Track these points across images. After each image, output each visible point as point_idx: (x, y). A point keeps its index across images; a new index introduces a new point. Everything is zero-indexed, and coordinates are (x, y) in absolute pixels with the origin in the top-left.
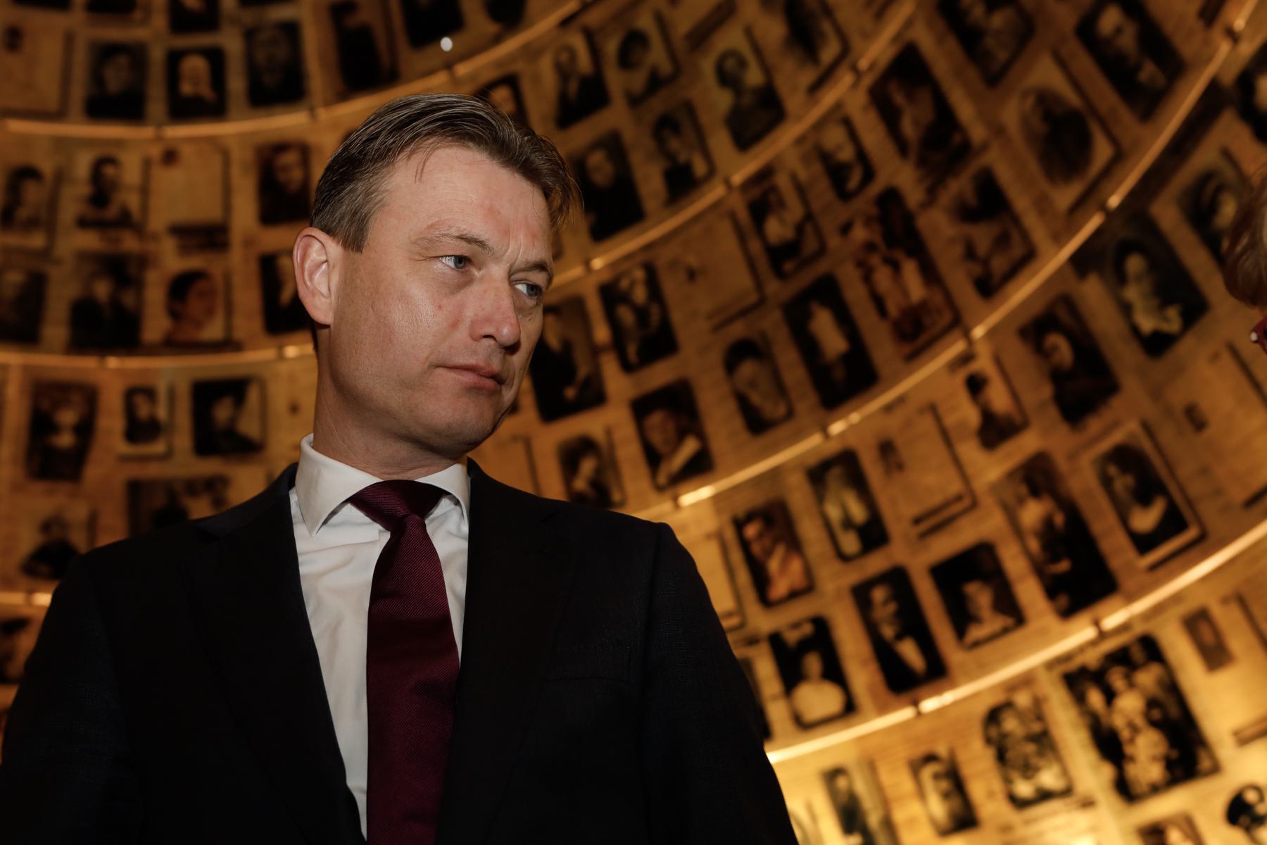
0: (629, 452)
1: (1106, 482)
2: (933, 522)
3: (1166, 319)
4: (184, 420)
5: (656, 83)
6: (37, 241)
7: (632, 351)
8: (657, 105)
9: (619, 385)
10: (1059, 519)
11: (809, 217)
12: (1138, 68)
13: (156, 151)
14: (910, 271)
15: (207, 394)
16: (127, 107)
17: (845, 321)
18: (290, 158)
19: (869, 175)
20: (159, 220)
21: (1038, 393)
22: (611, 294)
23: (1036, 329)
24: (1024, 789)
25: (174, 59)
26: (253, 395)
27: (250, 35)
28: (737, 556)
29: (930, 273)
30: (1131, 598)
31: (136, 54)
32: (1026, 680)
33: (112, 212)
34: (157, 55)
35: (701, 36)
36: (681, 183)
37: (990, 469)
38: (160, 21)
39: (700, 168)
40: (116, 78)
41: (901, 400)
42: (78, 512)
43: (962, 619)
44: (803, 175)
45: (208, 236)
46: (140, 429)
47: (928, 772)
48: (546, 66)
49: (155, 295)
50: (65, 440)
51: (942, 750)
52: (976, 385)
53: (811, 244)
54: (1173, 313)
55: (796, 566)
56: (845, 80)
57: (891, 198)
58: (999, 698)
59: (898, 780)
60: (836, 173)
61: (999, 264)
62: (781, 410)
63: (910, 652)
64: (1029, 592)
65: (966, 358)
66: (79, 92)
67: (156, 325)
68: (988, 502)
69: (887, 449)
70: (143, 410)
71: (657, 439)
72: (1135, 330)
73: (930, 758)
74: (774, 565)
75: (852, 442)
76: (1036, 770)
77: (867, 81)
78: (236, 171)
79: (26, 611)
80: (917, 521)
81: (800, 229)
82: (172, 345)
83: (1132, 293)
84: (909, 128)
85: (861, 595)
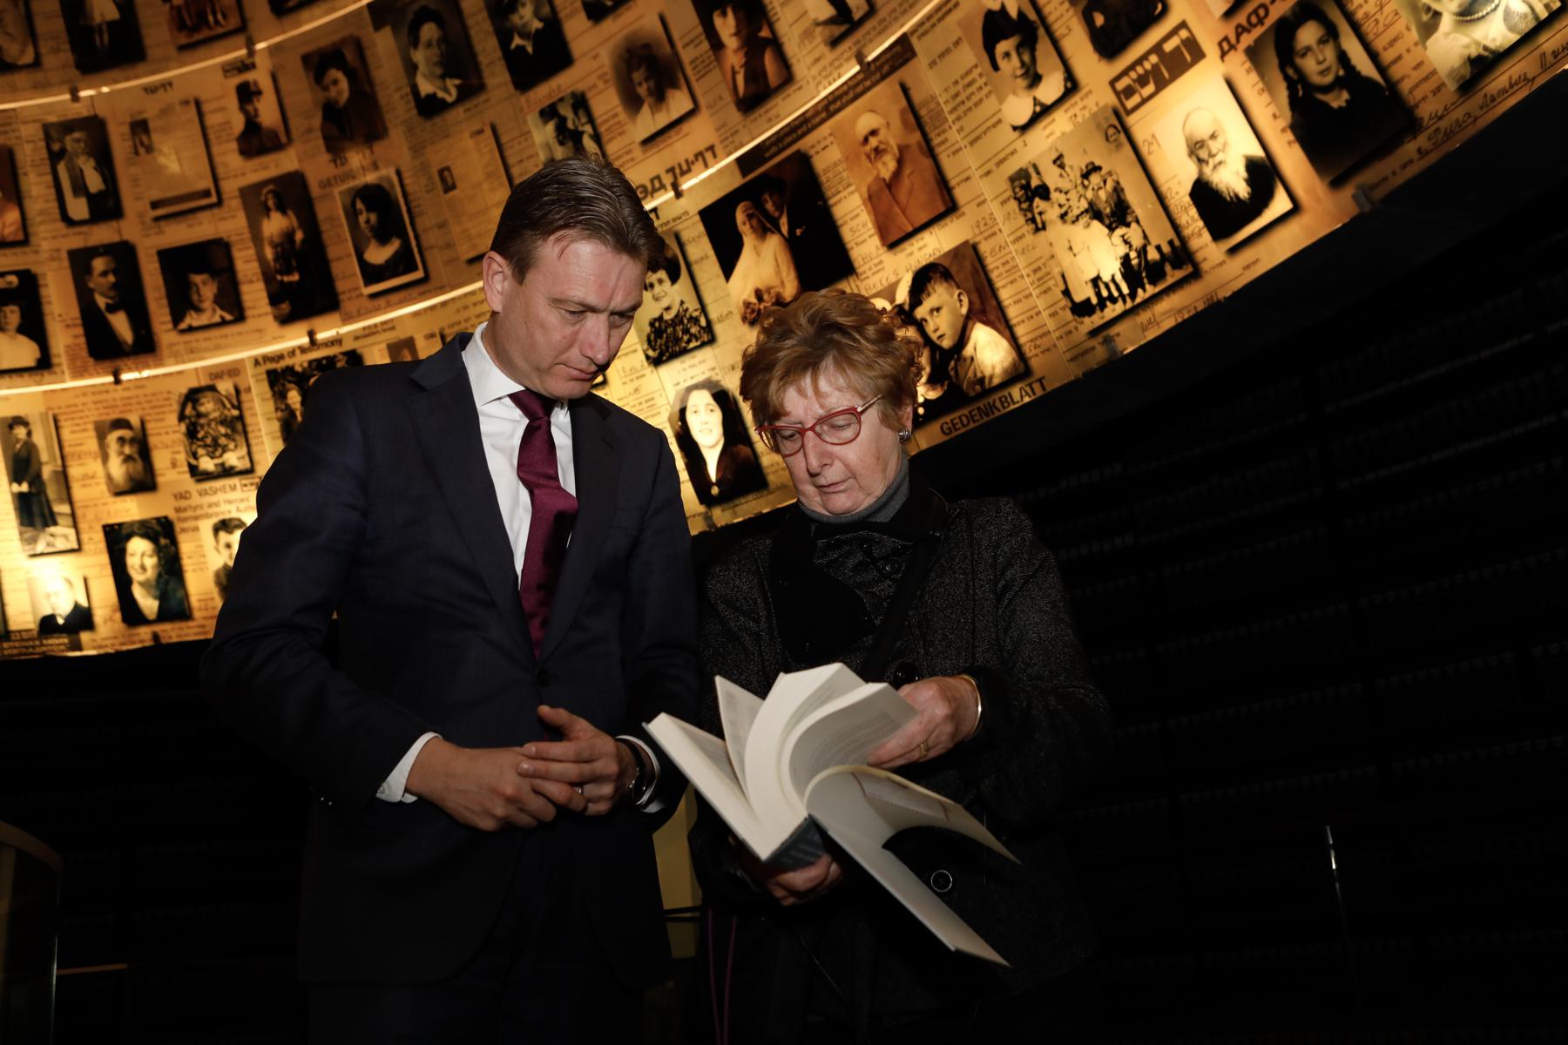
1: (352, 214)
2: (173, 208)
3: (446, 90)
10: (299, 236)
23: (320, 61)
24: (207, 464)
30: (348, 319)
32: (233, 371)
37: (241, 172)
41: (166, 85)
43: (181, 304)
47: (112, 437)
51: (134, 420)
52: (247, 94)
54: (452, 84)
58: (204, 382)
59: (81, 439)
62: (28, 58)
63: (121, 324)
64: (254, 294)
65: (245, 66)
68: (234, 203)
75: (102, 112)
76: (225, 450)
80: (155, 205)
85: (80, 261)
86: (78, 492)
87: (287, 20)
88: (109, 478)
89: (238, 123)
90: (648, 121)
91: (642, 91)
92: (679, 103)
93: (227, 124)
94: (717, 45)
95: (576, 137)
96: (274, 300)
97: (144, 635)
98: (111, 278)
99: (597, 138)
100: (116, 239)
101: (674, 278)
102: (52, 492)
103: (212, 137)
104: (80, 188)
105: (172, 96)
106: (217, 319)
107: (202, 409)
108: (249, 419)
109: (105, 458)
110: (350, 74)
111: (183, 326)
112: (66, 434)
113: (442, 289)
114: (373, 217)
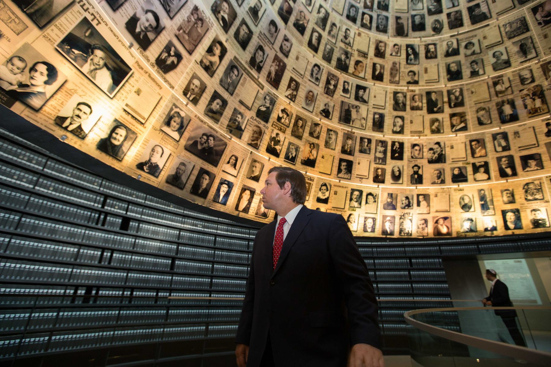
0: (447, 123)
4: (353, 92)
5: (474, 53)
7: (452, 104)
8: (473, 58)
9: (448, 110)
11: (510, 86)
15: (359, 87)
18: (382, 44)
19: (533, 81)
20: (355, 47)
22: (449, 93)
24: (530, 197)
26: (367, 91)
27: (378, 16)
28: (468, 147)
32: (540, 179)
33: (347, 41)
34: (361, 11)
36: (474, 74)
39: (481, 72)
42: (332, 104)
44: (511, 78)
47: (505, 193)
48: (445, 44)
49: (352, 63)
50: (332, 87)
51: (511, 189)
55: (483, 152)
58: (530, 181)
59: (497, 193)
60: (523, 80)
62: (489, 122)
63: (509, 171)
67: (351, 70)
70: (346, 87)
71: (454, 123)
74: (477, 151)
75: (506, 131)
76: (535, 195)
77: (541, 63)
78: (371, 43)
79: (319, 122)
80: (519, 147)
81: (507, 89)
82: (353, 75)
85: (499, 159)
86: (495, 203)
88: (503, 201)
97: (510, 232)
98: (507, 162)
100: (508, 154)
102: (489, 203)
103: (537, 133)
104: (500, 145)
106: (535, 169)
107: (529, 187)
108: (543, 188)
109: (502, 197)
111: (526, 170)
112: (493, 192)
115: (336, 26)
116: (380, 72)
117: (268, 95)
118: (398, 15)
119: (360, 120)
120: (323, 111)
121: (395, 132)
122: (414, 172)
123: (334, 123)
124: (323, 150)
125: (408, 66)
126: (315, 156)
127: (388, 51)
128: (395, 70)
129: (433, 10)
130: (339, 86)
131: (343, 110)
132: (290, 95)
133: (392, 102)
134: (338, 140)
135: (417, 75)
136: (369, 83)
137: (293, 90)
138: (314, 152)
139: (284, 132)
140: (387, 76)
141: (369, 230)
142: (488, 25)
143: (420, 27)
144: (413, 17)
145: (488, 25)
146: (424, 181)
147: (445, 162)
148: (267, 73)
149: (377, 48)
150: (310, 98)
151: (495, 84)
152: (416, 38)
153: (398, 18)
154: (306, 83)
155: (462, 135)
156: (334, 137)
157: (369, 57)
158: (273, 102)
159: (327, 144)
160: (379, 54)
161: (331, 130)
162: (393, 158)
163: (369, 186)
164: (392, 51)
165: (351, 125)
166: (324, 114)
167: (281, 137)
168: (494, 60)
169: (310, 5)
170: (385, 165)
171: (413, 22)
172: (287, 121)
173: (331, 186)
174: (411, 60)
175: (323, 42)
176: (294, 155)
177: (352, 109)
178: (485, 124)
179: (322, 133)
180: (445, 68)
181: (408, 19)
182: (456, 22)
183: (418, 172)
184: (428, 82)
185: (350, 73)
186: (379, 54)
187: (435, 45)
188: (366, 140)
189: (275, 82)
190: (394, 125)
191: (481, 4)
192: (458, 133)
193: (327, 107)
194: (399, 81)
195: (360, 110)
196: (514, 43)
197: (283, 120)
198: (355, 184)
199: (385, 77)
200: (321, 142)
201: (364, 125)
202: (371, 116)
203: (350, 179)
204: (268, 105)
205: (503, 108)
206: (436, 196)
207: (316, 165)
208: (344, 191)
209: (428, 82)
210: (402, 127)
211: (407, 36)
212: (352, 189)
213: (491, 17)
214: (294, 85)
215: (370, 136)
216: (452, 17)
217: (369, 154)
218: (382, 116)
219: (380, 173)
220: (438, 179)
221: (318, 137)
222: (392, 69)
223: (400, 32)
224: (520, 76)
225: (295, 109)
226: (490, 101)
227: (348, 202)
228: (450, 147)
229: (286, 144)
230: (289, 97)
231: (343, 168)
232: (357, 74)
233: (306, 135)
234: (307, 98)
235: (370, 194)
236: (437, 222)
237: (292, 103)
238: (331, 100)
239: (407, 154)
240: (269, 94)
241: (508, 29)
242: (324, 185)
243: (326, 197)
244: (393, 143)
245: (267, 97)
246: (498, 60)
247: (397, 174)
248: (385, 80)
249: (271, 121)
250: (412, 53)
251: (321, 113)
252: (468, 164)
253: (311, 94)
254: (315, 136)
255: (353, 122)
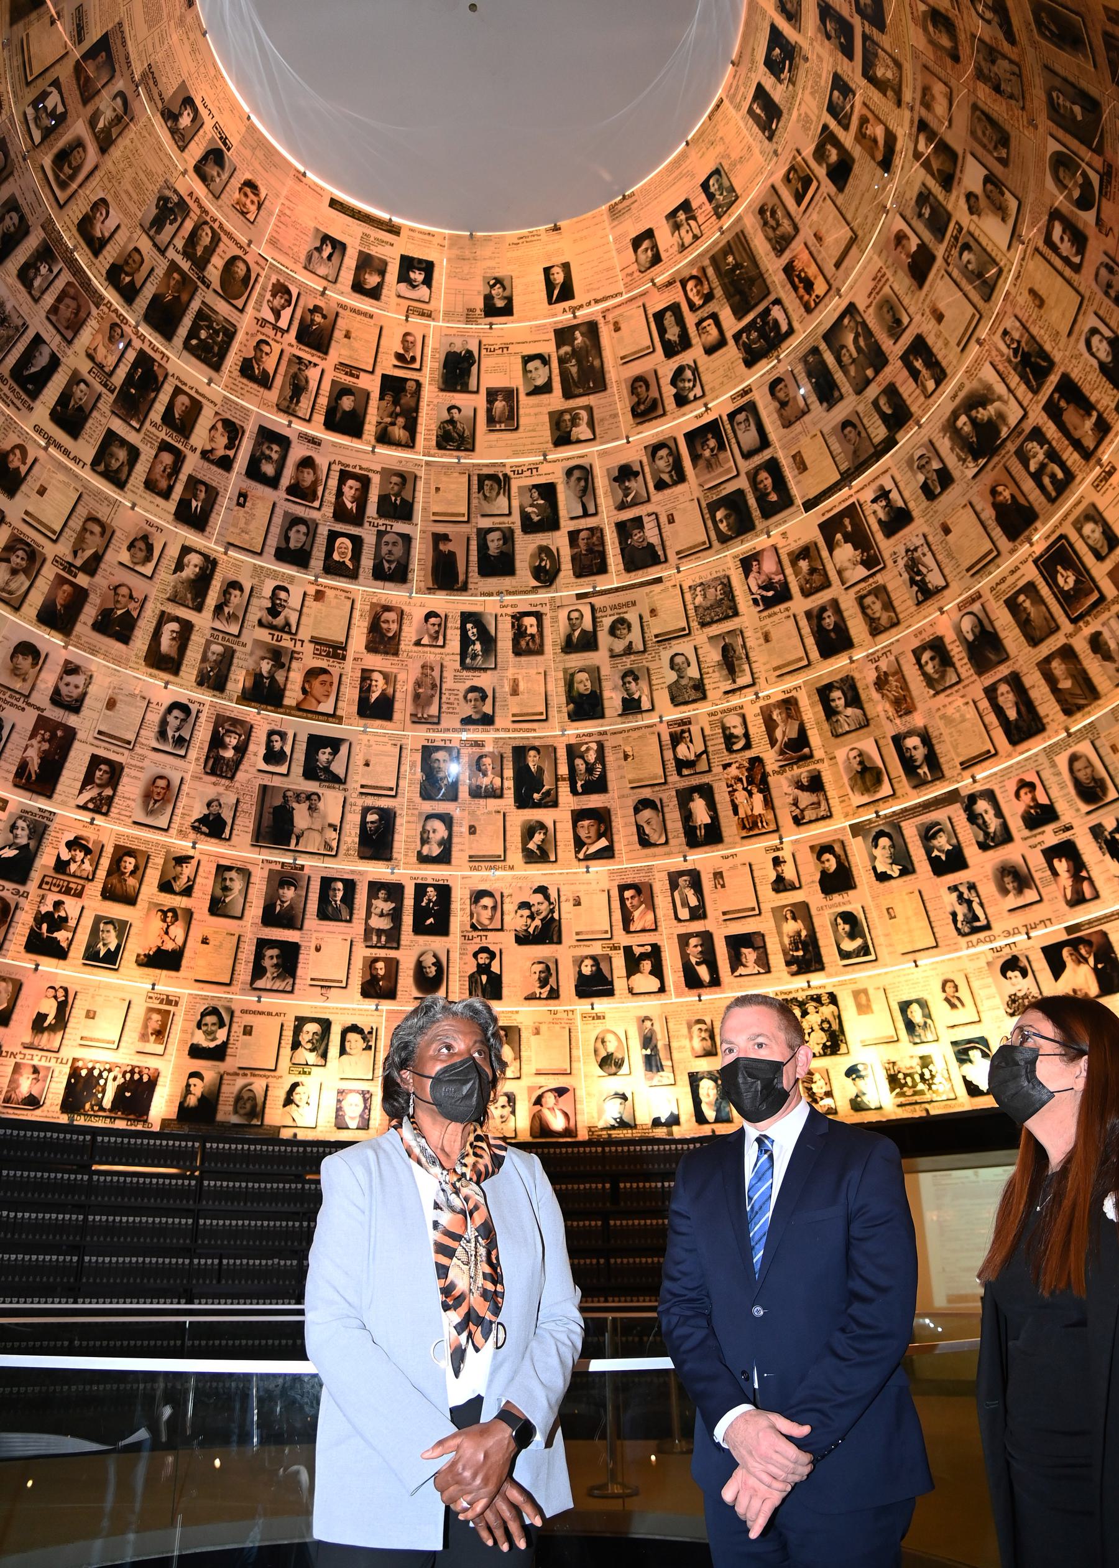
0: (565, 836)
1: (835, 925)
4: (300, 756)
6: (234, 629)
9: (568, 801)
10: (804, 933)
11: (705, 752)
12: (919, 767)
13: (312, 590)
14: (758, 798)
15: (316, 743)
16: (299, 558)
17: (712, 806)
18: (391, 616)
19: (748, 746)
20: (304, 634)
21: (811, 872)
22: (573, 752)
25: (333, 536)
26: (344, 749)
27: (380, 534)
29: (769, 803)
30: (829, 976)
31: (311, 528)
33: (279, 621)
34: (323, 531)
35: (664, 639)
36: (631, 706)
37: (771, 900)
38: (328, 510)
40: (297, 539)
42: (229, 799)
43: (736, 962)
45: (336, 650)
46: (273, 756)
49: (296, 677)
50: (229, 754)
51: (708, 1021)
52: (777, 862)
53: (703, 766)
56: (747, 697)
57: (756, 762)
59: (679, 1028)
60: (729, 739)
61: (809, 815)
62: (663, 840)
63: (703, 972)
64: (777, 959)
66: (273, 542)
67: (292, 696)
68: (767, 915)
69: (718, 875)
70: (277, 746)
72: (874, 869)
73: (699, 1021)
74: (636, 914)
77: (762, 703)
78: (357, 614)
79: (191, 853)
80: (724, 913)
81: (699, 756)
82: (300, 709)
83: (877, 852)
84: (778, 734)
86: (675, 1055)
87: (802, 828)
88: (693, 1048)
89: (773, 876)
90: (1012, 901)
91: (1010, 887)
92: (1030, 895)
93: (764, 877)
94: (1055, 873)
95: (969, 903)
96: (788, 964)
97: (706, 1130)
99: (981, 904)
101: (1024, 974)
102: (663, 1054)
104: (685, 903)
105: (737, 861)
109: (691, 1038)
110: (837, 857)
113: (885, 965)
114: (847, 927)
115: (241, 590)
116: (383, 694)
117: (20, 817)
118: (441, 529)
119: (321, 831)
120: (204, 820)
121: (423, 859)
122: (479, 965)
123: (240, 849)
124: (205, 923)
125: (465, 673)
126: (180, 941)
127: (409, 633)
128: (427, 690)
129: (536, 519)
130: (252, 747)
131: (268, 810)
132: (91, 800)
133: (419, 775)
134: (250, 891)
135: (489, 701)
136: (351, 728)
137: (99, 786)
138: (177, 931)
139: (79, 895)
140: (403, 706)
141: (353, 1124)
142: (659, 580)
143: (498, 564)
144: (483, 534)
145: (659, 580)
146: (505, 992)
147: (559, 942)
148: (14, 769)
149: (375, 627)
150: (159, 795)
151: (676, 739)
152: (490, 594)
153: (439, 539)
154: (143, 758)
155: (599, 868)
156: (237, 885)
157: (350, 654)
158: (39, 829)
159: (217, 907)
160: (382, 640)
161: (229, 868)
162: (419, 929)
163: (349, 1007)
164: (419, 632)
165: (292, 847)
166: (204, 829)
167: (71, 907)
168: (672, 676)
169: (148, 559)
170: (397, 948)
171: (483, 547)
172: (87, 866)
173: (232, 1014)
174: (474, 656)
175: (197, 641)
176: (113, 948)
177: (295, 805)
178: (655, 845)
179: (198, 880)
180: (562, 683)
181: (468, 539)
182: (590, 562)
183: (489, 965)
184: (520, 719)
185: (290, 707)
186: (382, 640)
187: (538, 616)
188: (340, 885)
189: (42, 779)
190: (424, 841)
191: (646, 519)
192: (590, 863)
193: (214, 809)
194: (439, 717)
195: (321, 805)
196: (710, 638)
197: (73, 867)
198: (306, 1003)
199: (397, 706)
200: (199, 902)
201: (334, 844)
202: (353, 820)
203: (292, 992)
204: (23, 841)
205: (692, 805)
206: (537, 1032)
207: (184, 962)
208: (274, 1023)
209: (520, 719)
210: (447, 845)
211: (464, 588)
212: (297, 1018)
213: (666, 561)
214: (105, 775)
215: (353, 872)
216: (582, 543)
217: (350, 921)
218: (387, 818)
219: (381, 972)
220: (542, 987)
221: (188, 892)
222: (418, 684)
223: (446, 575)
224: (724, 728)
225: (110, 831)
226: (665, 783)
227: (286, 1051)
228: (572, 902)
229: (87, 923)
230: (91, 806)
231: (267, 963)
232: (311, 705)
233: (149, 889)
234: (147, 796)
235: (354, 1029)
236: (538, 1101)
237: (100, 820)
238: (227, 788)
239: (458, 920)
240: (24, 814)
241: (699, 600)
242: (209, 1014)
243: (218, 1042)
244: (420, 889)
245: (20, 823)
246: (680, 677)
247: (432, 971)
248: (397, 716)
249: (36, 876)
250: (477, 635)
251: (194, 828)
252: (615, 948)
253: (162, 783)
254: (177, 889)
255: (298, 838)
